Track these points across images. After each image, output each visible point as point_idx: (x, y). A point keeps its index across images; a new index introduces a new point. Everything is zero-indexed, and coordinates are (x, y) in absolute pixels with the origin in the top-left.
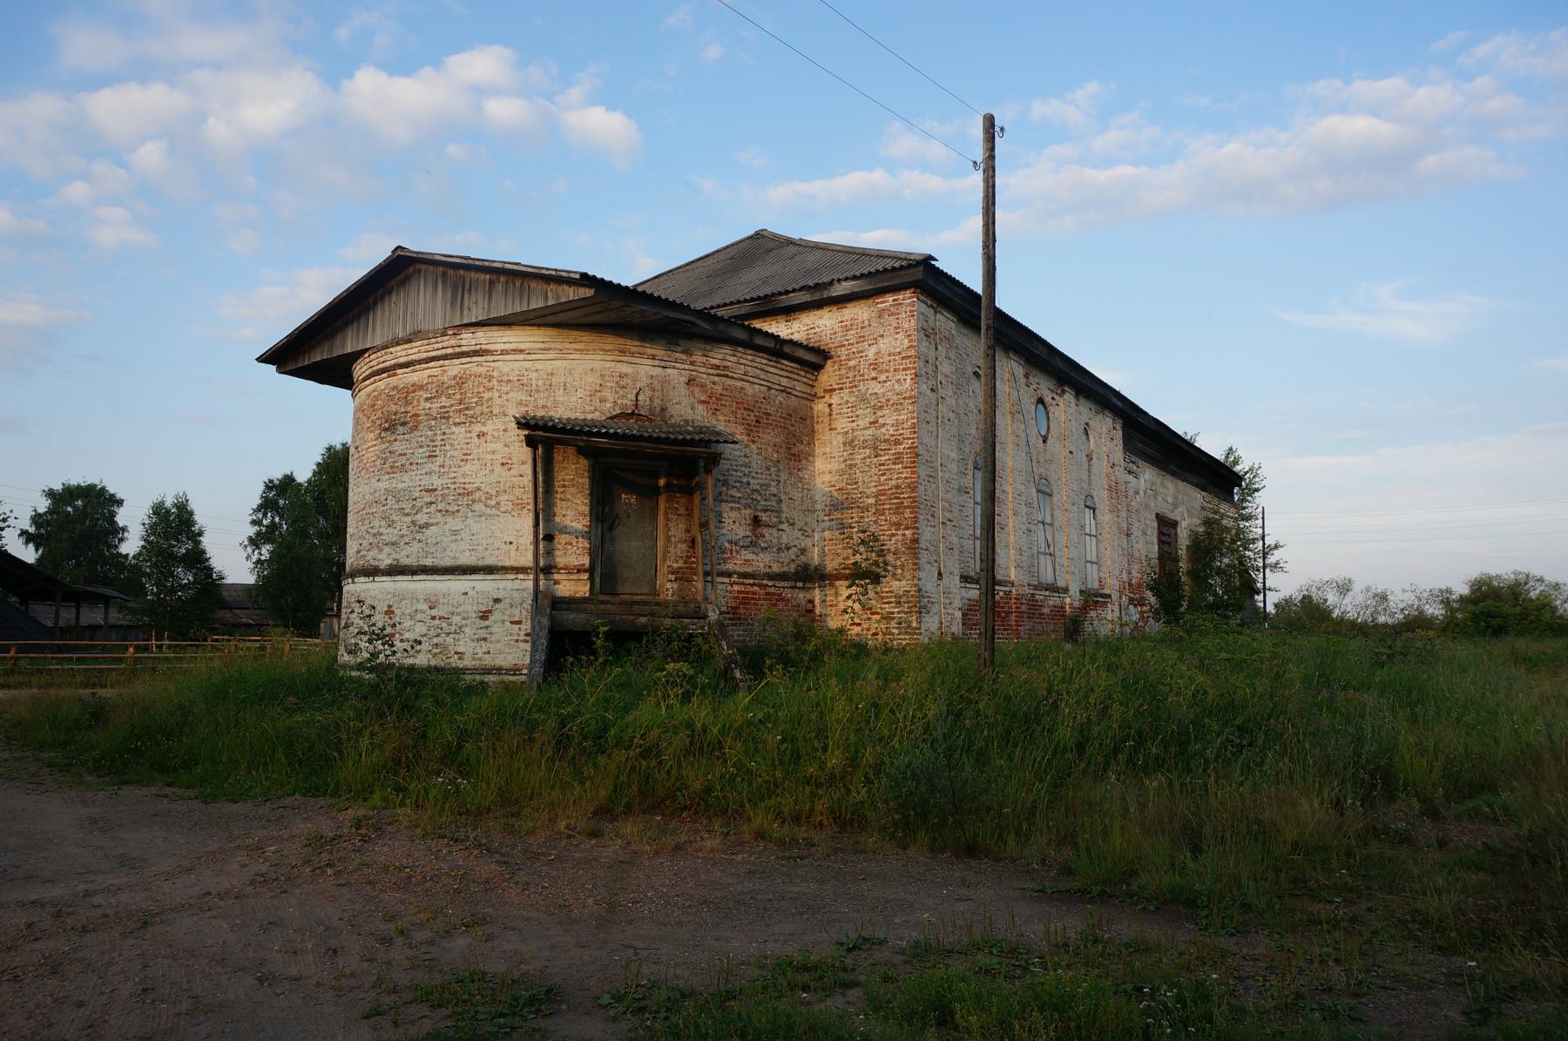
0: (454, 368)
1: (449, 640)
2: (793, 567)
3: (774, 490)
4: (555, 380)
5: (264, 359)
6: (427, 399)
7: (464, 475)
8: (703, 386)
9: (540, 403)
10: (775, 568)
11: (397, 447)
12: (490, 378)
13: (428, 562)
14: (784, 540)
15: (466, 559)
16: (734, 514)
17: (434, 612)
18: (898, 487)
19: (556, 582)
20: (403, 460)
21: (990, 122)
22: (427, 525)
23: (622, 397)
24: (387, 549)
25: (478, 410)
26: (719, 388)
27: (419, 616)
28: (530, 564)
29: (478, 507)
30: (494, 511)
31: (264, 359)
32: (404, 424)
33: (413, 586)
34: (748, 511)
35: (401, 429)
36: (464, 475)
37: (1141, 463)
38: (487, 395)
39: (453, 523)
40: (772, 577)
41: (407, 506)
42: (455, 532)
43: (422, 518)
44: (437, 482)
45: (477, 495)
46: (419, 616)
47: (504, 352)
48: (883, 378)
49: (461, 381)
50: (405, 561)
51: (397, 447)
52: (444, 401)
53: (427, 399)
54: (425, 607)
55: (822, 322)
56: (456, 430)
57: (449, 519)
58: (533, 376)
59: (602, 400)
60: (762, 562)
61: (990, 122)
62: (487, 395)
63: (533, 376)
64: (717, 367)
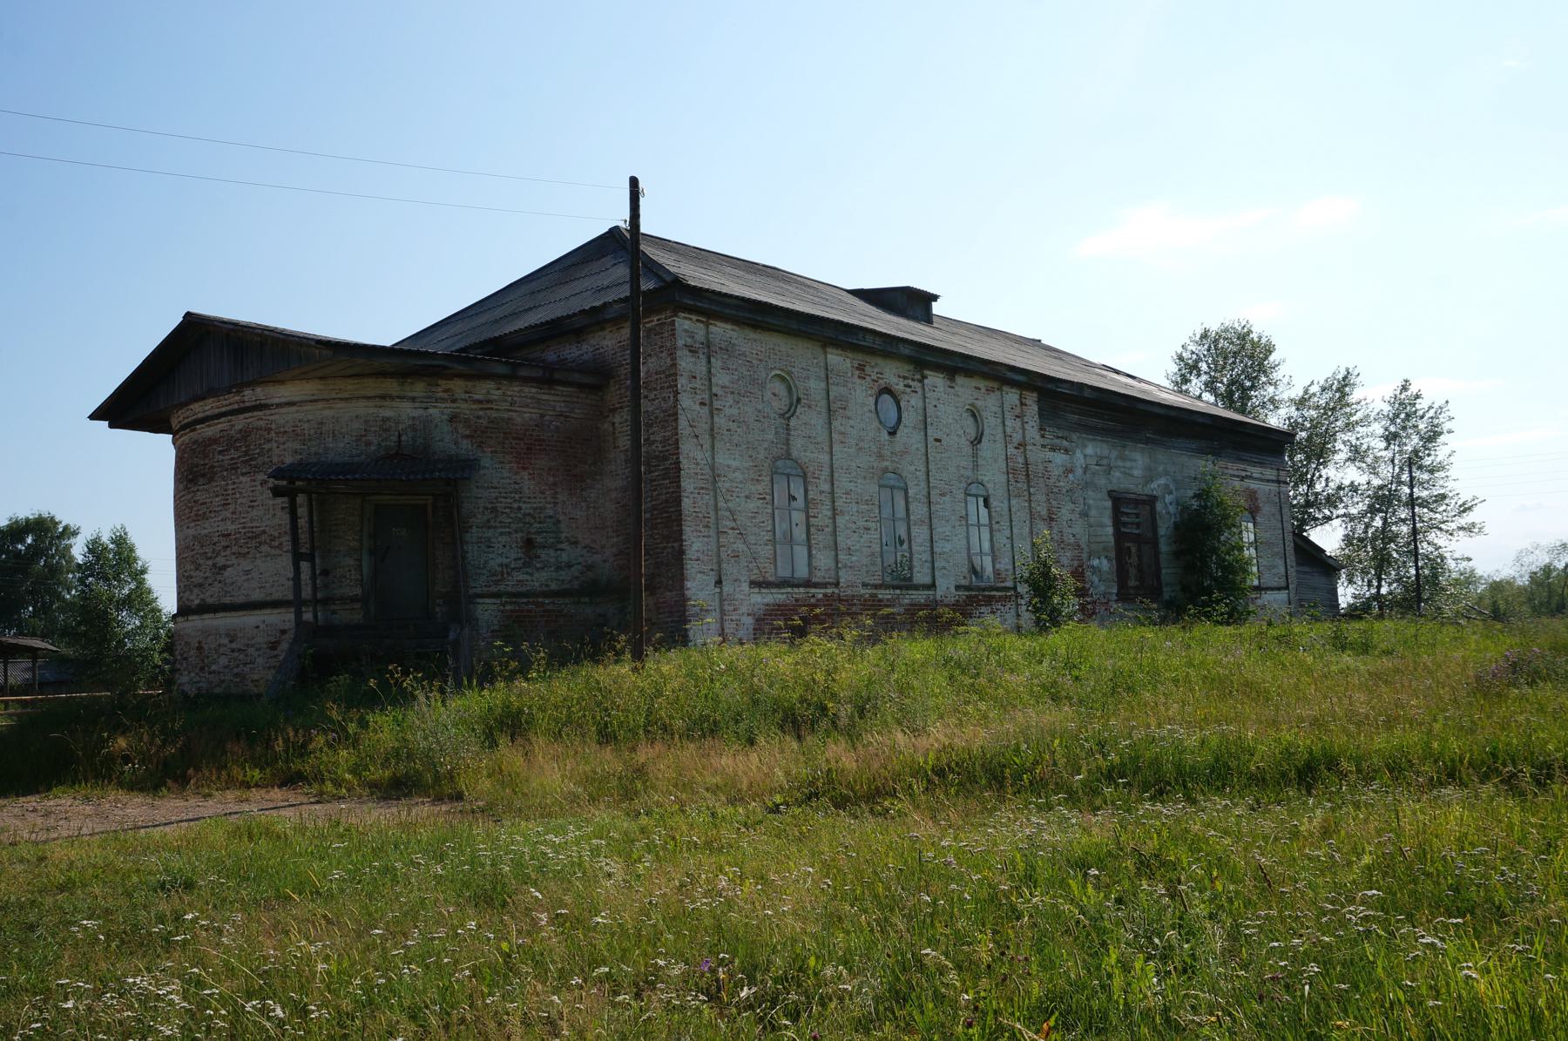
0: (240, 422)
1: (247, 669)
2: (576, 584)
3: (551, 513)
4: (324, 429)
5: (93, 417)
6: (220, 452)
7: (252, 520)
8: (467, 421)
9: (313, 450)
10: (554, 586)
11: (201, 497)
12: (269, 430)
13: (227, 600)
14: (564, 557)
15: (257, 596)
16: (503, 539)
17: (234, 645)
18: (667, 501)
19: (334, 612)
20: (203, 509)
21: (634, 182)
22: (225, 567)
23: (385, 440)
24: (196, 591)
25: (260, 460)
26: (484, 422)
27: (222, 650)
28: (291, 597)
29: (265, 548)
30: (278, 552)
31: (93, 417)
32: (203, 475)
33: (215, 623)
34: (519, 535)
35: (201, 481)
36: (252, 520)
37: (1074, 436)
38: (266, 447)
39: (246, 564)
40: (545, 595)
41: (209, 550)
42: (247, 572)
43: (220, 561)
44: (231, 527)
45: (263, 537)
46: (222, 650)
47: (279, 405)
48: (652, 396)
49: (245, 434)
50: (210, 601)
51: (201, 497)
52: (233, 454)
53: (220, 452)
54: (225, 641)
55: (605, 343)
56: (243, 479)
57: (241, 560)
58: (306, 426)
59: (368, 444)
60: (539, 579)
61: (634, 182)
62: (266, 447)
63: (306, 426)
64: (480, 402)
